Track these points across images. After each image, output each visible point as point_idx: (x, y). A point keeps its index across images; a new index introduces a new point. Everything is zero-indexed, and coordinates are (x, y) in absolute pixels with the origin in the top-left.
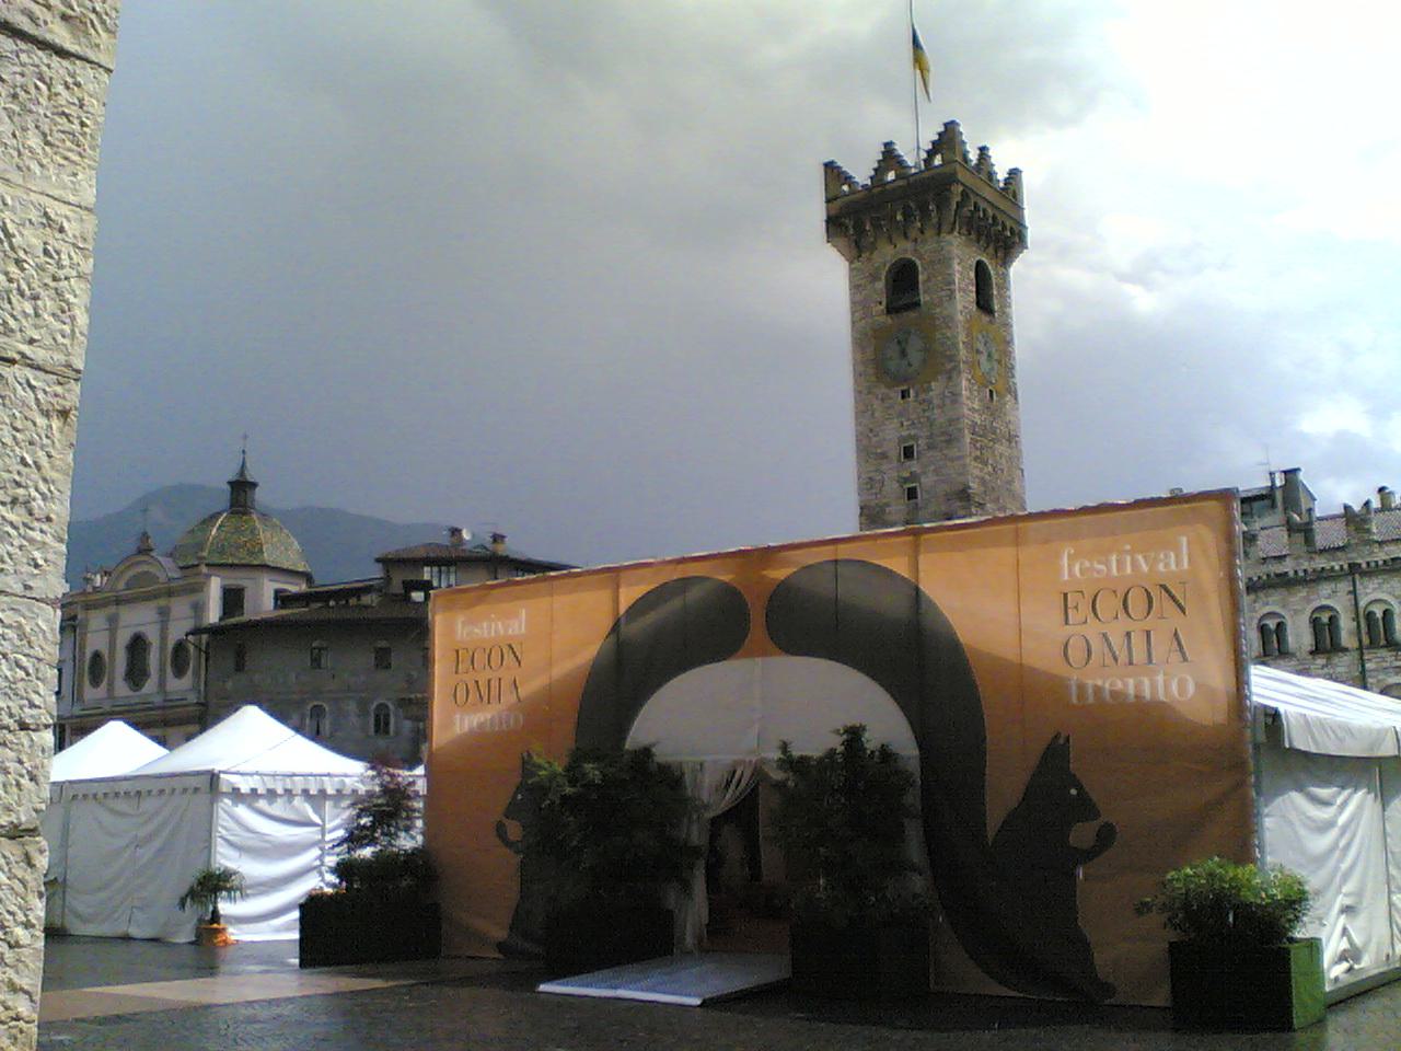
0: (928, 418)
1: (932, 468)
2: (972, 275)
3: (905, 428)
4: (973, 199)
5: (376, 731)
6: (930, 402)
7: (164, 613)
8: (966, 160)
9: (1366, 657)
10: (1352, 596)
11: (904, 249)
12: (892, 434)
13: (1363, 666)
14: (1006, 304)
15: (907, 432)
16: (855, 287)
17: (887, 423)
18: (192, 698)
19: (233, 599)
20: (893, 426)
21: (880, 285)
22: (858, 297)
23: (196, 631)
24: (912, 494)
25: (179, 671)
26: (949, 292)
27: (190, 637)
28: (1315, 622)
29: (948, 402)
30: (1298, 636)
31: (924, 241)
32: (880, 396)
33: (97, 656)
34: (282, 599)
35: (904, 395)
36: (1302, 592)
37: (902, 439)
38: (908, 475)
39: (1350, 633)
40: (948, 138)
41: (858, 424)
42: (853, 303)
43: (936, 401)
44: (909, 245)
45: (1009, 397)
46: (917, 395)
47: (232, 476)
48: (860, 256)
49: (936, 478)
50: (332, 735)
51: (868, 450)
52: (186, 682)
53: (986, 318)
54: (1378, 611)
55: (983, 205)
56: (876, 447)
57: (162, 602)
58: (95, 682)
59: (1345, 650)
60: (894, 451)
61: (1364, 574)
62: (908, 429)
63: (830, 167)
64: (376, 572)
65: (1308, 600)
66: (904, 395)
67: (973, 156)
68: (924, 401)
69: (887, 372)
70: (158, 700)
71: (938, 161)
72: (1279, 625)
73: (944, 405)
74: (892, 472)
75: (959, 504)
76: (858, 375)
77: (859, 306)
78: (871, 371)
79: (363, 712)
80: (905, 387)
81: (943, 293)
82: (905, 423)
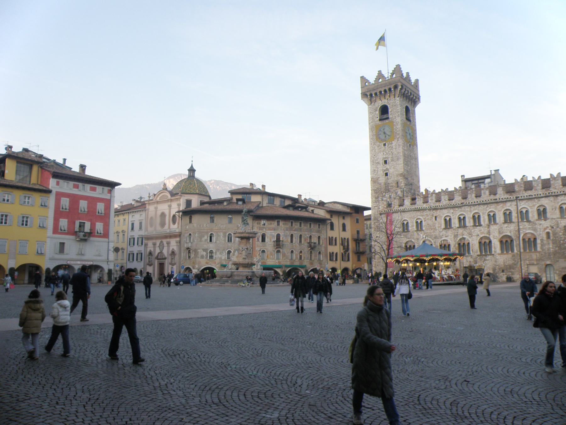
2: (404, 110)
4: (404, 87)
5: (228, 241)
6: (392, 147)
7: (170, 206)
8: (402, 75)
9: (520, 224)
10: (516, 206)
11: (384, 102)
12: (381, 157)
13: (519, 227)
14: (414, 119)
16: (370, 113)
18: (177, 231)
19: (189, 203)
21: (378, 112)
22: (371, 116)
23: (178, 212)
24: (386, 174)
25: (174, 223)
27: (177, 213)
28: (505, 214)
29: (397, 147)
30: (500, 218)
31: (390, 100)
33: (151, 218)
34: (202, 203)
35: (385, 145)
36: (501, 205)
37: (384, 158)
39: (515, 217)
40: (398, 69)
41: (371, 153)
42: (369, 118)
43: (394, 147)
44: (386, 101)
45: (415, 147)
46: (388, 145)
47: (189, 167)
50: (216, 242)
51: (374, 162)
52: (176, 226)
53: (409, 123)
54: (524, 211)
55: (407, 89)
57: (169, 203)
58: (151, 226)
59: (514, 222)
60: (382, 162)
61: (520, 200)
63: (362, 78)
64: (229, 195)
65: (503, 207)
66: (385, 145)
67: (405, 75)
69: (379, 138)
70: (168, 231)
71: (394, 76)
72: (494, 214)
74: (381, 168)
76: (371, 139)
77: (371, 119)
78: (375, 137)
79: (225, 236)
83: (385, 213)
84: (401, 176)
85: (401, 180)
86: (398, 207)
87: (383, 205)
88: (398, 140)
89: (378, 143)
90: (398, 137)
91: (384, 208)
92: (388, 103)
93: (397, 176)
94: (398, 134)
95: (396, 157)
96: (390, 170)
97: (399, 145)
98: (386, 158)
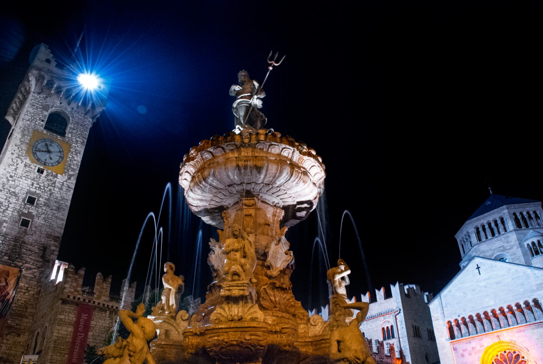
0: (50, 190)
1: (43, 216)
3: (34, 187)
6: (55, 183)
15: (34, 190)
17: (24, 178)
20: (26, 182)
21: (47, 114)
24: (25, 223)
26: (82, 141)
32: (24, 163)
35: (40, 171)
38: (26, 212)
46: (48, 175)
48: (40, 94)
49: (44, 223)
56: (10, 187)
60: (22, 196)
62: (36, 189)
66: (40, 171)
68: (51, 180)
73: (61, 189)
75: (53, 242)
80: (42, 167)
81: (79, 140)
82: (35, 185)
83: (77, 305)
84: (55, 241)
85: (53, 248)
86: (108, 299)
87: (74, 284)
88: (69, 179)
89: (28, 161)
90: (71, 173)
91: (76, 291)
92: (72, 114)
93: (48, 236)
94: (73, 170)
95: (56, 202)
96: (36, 219)
97: (68, 187)
98: (34, 193)
